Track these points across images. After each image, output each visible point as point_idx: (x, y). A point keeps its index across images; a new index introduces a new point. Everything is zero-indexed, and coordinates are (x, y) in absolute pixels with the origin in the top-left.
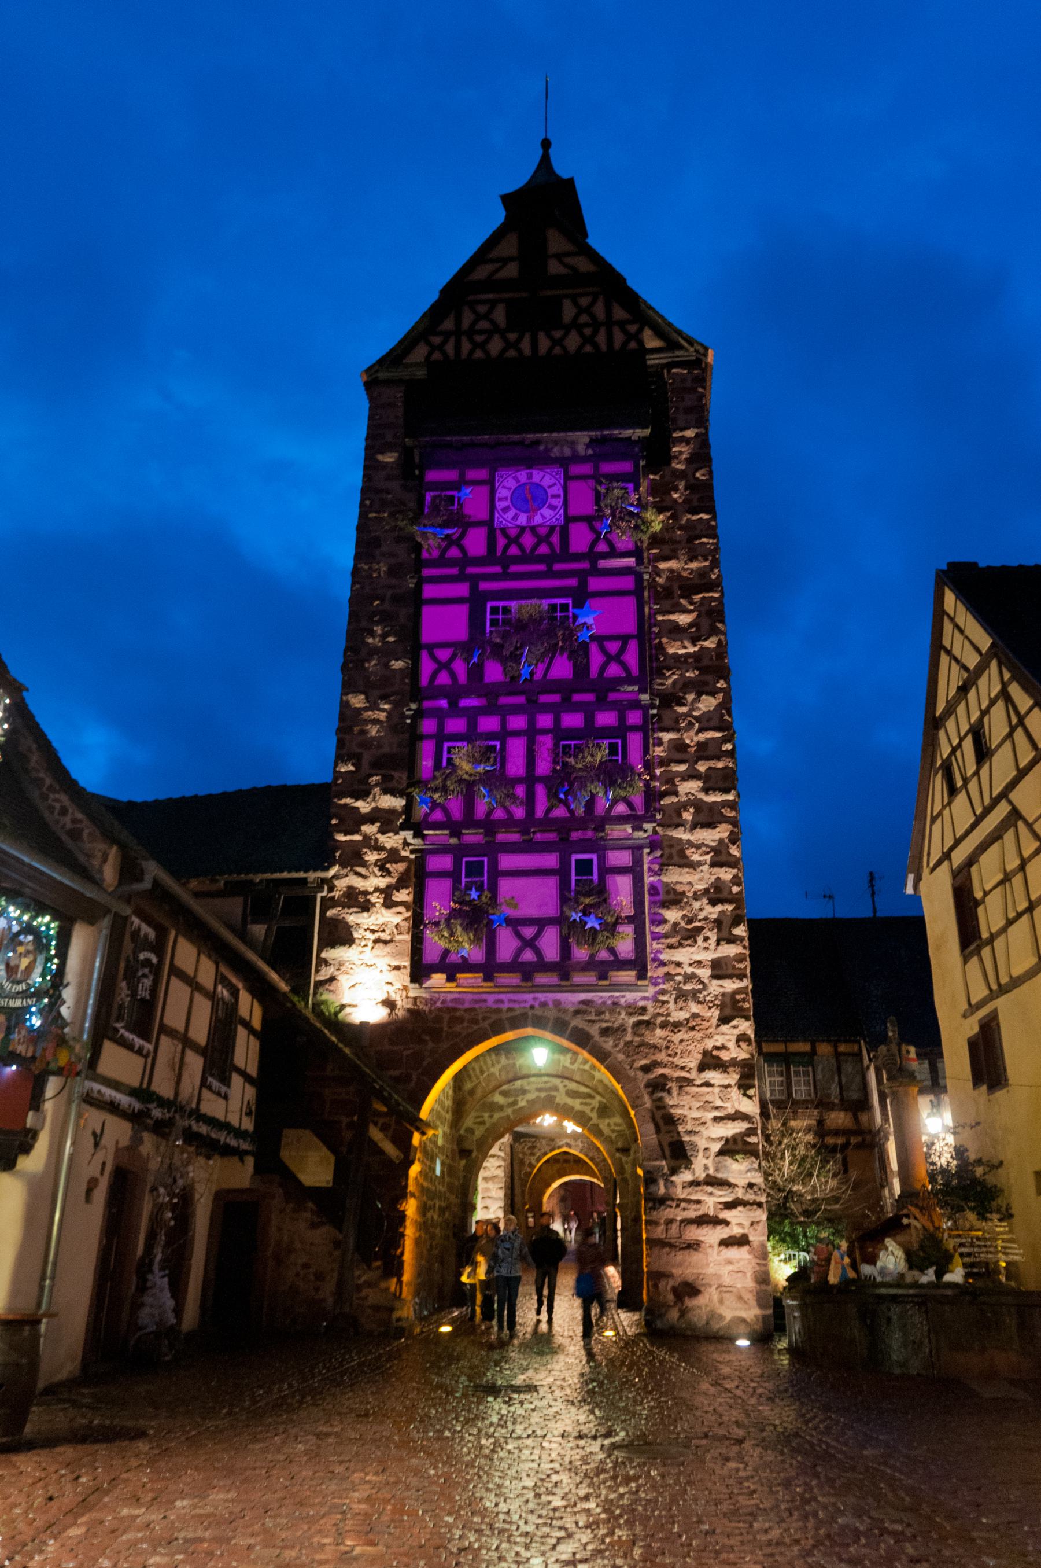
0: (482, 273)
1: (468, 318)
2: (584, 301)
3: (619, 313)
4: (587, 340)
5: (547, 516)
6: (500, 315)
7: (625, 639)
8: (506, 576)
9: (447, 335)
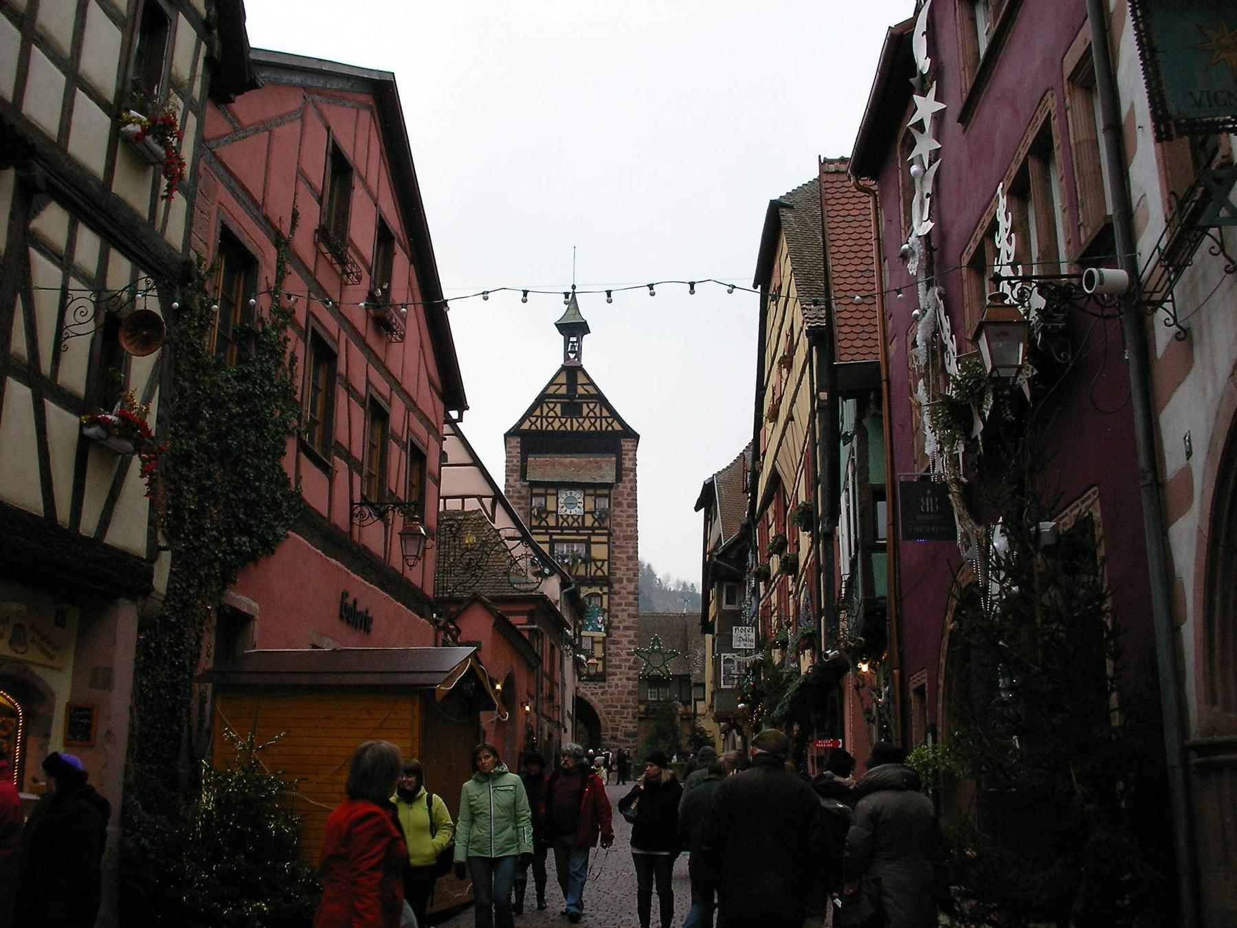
0: (551, 390)
1: (546, 410)
2: (592, 406)
3: (605, 413)
4: (593, 424)
5: (577, 511)
6: (558, 409)
7: (603, 561)
8: (562, 534)
9: (537, 417)
